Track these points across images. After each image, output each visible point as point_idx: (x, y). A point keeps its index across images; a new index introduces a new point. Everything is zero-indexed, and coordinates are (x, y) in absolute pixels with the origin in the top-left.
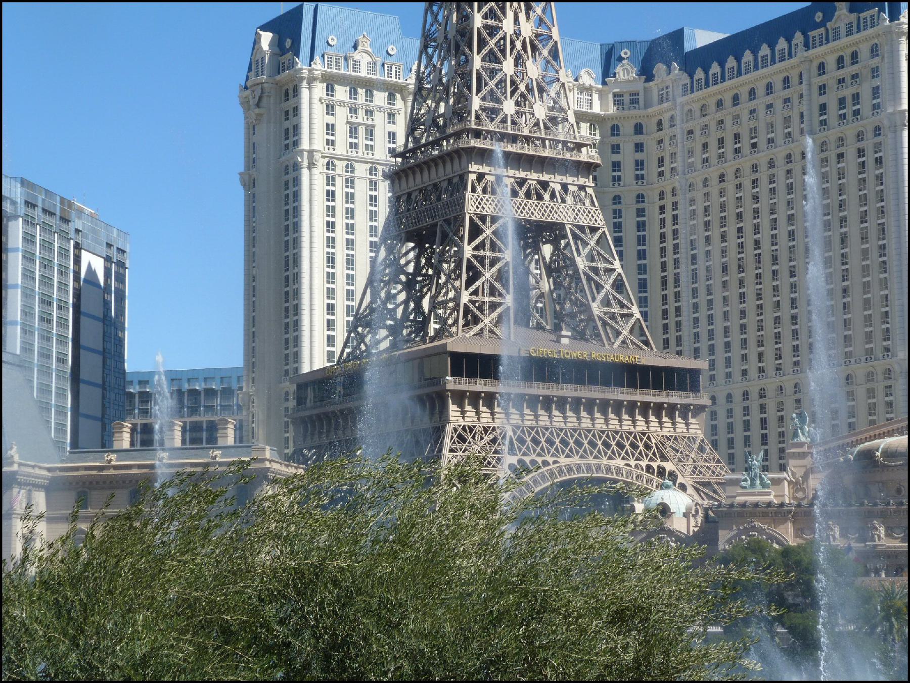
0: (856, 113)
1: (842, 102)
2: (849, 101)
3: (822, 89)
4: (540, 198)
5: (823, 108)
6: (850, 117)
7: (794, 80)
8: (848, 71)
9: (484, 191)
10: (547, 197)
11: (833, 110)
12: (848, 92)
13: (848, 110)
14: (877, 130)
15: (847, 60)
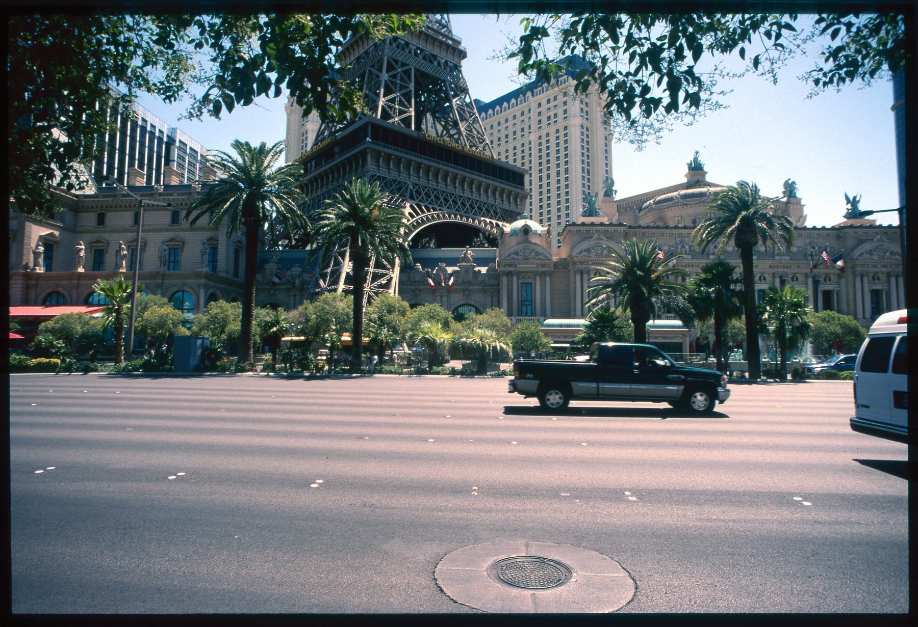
0: (556, 122)
1: (549, 118)
2: (552, 117)
3: (540, 114)
4: (431, 62)
5: (540, 122)
6: (552, 124)
7: (526, 112)
8: (553, 103)
9: (398, 47)
10: (436, 63)
11: (545, 121)
12: (552, 114)
13: (552, 120)
14: (566, 128)
15: (552, 100)
